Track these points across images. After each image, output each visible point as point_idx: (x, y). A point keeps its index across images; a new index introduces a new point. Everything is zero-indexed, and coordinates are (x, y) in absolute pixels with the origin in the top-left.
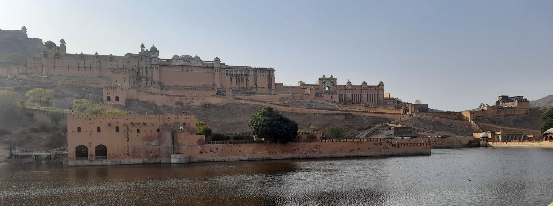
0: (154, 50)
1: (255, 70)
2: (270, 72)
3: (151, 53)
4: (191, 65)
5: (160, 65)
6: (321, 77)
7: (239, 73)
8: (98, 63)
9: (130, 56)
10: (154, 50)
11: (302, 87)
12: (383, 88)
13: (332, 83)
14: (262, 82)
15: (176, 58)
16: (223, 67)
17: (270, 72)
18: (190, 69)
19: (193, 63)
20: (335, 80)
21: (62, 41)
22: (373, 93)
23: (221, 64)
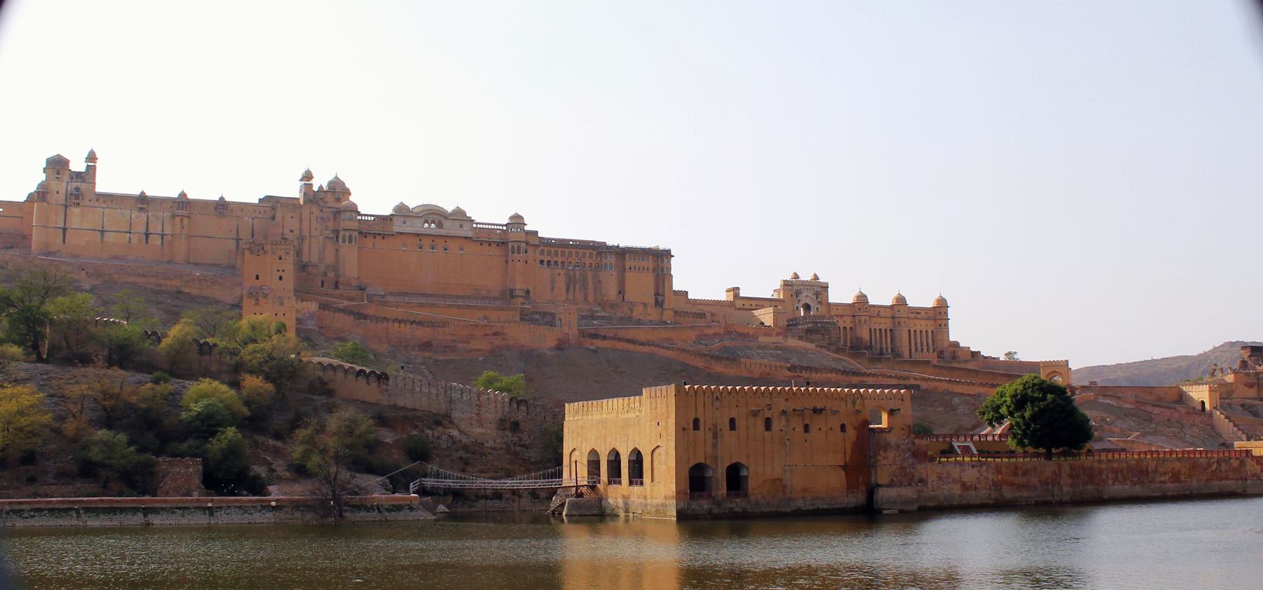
0: (338, 190)
1: (622, 253)
2: (659, 259)
3: (330, 198)
4: (442, 232)
5: (360, 233)
6: (789, 277)
7: (574, 260)
8: (186, 220)
9: (271, 203)
10: (338, 190)
11: (739, 304)
12: (946, 313)
13: (817, 294)
14: (640, 287)
15: (402, 211)
16: (533, 242)
17: (659, 259)
18: (440, 244)
19: (450, 228)
20: (825, 287)
21: (92, 157)
22: (920, 325)
23: (528, 233)
